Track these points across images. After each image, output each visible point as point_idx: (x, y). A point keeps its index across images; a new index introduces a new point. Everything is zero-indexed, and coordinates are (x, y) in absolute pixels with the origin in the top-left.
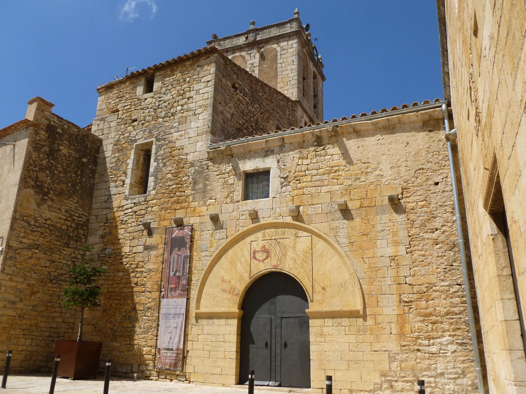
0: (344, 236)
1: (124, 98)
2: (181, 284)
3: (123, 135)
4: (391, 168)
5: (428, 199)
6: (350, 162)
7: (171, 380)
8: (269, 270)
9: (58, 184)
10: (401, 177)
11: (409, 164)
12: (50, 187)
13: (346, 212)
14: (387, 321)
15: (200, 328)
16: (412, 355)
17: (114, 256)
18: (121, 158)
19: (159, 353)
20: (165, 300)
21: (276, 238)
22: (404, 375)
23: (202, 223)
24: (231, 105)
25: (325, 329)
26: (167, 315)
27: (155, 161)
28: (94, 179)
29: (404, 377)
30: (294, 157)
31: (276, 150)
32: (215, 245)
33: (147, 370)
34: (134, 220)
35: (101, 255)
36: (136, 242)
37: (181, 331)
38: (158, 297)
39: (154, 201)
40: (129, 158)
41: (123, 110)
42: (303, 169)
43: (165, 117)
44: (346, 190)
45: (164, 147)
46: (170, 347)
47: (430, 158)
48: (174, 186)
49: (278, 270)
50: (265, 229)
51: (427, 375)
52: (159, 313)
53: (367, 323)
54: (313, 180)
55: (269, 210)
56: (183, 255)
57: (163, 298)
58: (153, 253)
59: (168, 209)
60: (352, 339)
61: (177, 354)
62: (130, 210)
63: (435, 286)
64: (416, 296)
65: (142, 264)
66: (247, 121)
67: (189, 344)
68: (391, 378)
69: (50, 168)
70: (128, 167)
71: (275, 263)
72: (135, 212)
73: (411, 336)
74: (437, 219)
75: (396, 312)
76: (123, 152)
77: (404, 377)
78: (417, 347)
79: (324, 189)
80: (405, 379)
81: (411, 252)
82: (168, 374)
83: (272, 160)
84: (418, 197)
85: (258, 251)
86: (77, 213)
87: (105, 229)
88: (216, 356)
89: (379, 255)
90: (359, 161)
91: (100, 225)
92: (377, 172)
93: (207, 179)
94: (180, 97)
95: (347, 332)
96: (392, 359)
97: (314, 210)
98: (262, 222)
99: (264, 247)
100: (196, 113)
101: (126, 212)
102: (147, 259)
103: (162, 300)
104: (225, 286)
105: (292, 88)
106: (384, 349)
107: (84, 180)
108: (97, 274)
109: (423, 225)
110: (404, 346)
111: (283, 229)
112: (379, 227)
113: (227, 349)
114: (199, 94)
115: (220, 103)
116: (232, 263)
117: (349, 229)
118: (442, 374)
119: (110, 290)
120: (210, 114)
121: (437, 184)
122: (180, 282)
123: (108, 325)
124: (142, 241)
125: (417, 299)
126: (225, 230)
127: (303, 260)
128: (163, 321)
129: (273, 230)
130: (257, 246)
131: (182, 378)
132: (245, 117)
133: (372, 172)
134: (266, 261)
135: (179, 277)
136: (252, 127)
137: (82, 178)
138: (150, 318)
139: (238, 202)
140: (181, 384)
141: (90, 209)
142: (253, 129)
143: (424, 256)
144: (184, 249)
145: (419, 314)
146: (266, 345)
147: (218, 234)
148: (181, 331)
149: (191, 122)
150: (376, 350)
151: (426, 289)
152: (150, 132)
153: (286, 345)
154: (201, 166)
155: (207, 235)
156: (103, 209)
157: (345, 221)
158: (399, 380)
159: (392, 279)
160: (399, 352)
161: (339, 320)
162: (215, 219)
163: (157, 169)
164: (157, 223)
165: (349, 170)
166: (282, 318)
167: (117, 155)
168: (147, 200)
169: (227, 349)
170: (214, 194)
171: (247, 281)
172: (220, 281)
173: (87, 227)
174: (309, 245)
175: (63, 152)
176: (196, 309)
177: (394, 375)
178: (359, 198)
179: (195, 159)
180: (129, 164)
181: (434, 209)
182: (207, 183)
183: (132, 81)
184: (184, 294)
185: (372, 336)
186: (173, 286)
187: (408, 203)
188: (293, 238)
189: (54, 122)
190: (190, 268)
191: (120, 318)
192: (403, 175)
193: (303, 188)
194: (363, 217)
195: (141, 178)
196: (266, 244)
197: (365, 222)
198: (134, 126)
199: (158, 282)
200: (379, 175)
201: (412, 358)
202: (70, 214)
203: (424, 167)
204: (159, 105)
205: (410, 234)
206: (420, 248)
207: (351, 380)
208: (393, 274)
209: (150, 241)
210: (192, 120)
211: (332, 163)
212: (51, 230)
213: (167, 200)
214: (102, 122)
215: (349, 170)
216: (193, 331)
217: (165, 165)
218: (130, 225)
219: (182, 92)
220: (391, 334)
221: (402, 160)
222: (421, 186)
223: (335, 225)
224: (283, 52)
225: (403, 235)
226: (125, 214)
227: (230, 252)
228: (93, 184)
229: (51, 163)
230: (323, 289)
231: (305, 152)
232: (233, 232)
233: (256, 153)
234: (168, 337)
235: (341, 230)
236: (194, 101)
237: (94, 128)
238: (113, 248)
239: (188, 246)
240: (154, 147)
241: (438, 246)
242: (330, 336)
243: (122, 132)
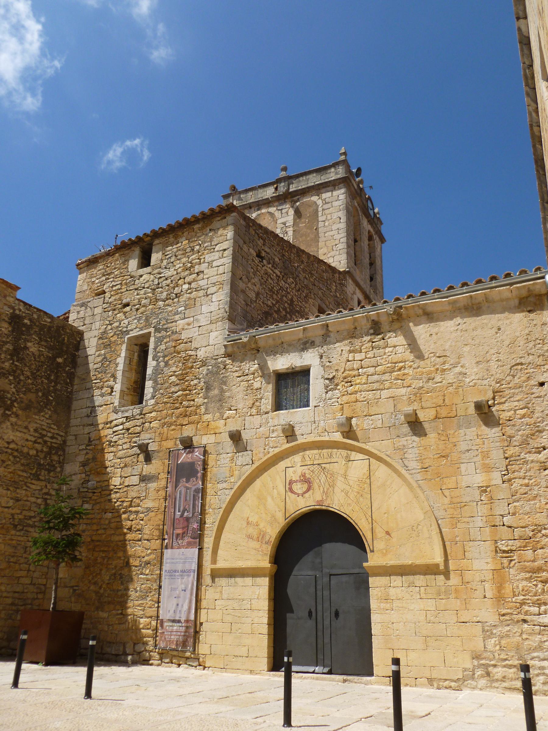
0: (414, 459)
1: (113, 276)
2: (190, 528)
3: (111, 324)
4: (477, 362)
5: (530, 405)
6: (420, 356)
7: (179, 665)
8: (312, 507)
9: (24, 394)
10: (492, 375)
11: (501, 357)
12: (14, 399)
13: (416, 426)
14: (478, 579)
15: (218, 590)
16: (516, 629)
17: (100, 490)
18: (108, 356)
19: (162, 626)
20: (169, 551)
21: (320, 462)
22: (505, 657)
23: (218, 443)
24: (256, 280)
27: (153, 360)
28: (72, 386)
29: (506, 660)
30: (342, 350)
31: (318, 341)
32: (236, 473)
34: (126, 440)
35: (82, 490)
36: (128, 470)
38: (160, 547)
40: (119, 356)
41: (111, 292)
42: (355, 367)
43: (167, 299)
44: (415, 394)
45: (165, 340)
46: (177, 618)
47: (531, 349)
48: (180, 393)
49: (324, 508)
50: (305, 450)
51: (538, 657)
52: (161, 569)
53: (451, 582)
54: (369, 381)
55: (310, 424)
57: (166, 548)
58: (153, 485)
59: (171, 424)
60: (430, 604)
61: (187, 627)
62: (121, 427)
63: (545, 529)
64: (518, 543)
65: (137, 501)
66: (277, 302)
67: (203, 612)
68: (488, 662)
69: (15, 372)
70: (118, 369)
72: (128, 429)
73: (514, 600)
74: (544, 434)
75: (491, 566)
76: (111, 348)
77: (506, 660)
78: (522, 617)
79: (385, 394)
80: (507, 662)
81: (510, 480)
82: (175, 656)
83: (313, 354)
84: (516, 404)
85: (296, 482)
86: (50, 432)
87: (87, 453)
88: (240, 631)
89: (464, 484)
90: (432, 355)
91: (81, 448)
92: (458, 369)
93: (225, 383)
94: (187, 272)
95: (423, 595)
96: (487, 634)
97: (371, 422)
98: (301, 440)
99: (304, 475)
100: (208, 293)
101: (115, 429)
102: (144, 494)
103: (165, 551)
104: (251, 530)
105: (339, 254)
106: (476, 620)
107: (59, 387)
108: (77, 516)
109: (525, 443)
110: (504, 615)
111: (330, 450)
112: (463, 446)
113: (256, 620)
114: (212, 267)
115: (241, 279)
116: (261, 498)
117: (421, 448)
119: (94, 538)
120: (227, 294)
121: (542, 384)
122: (189, 526)
123: (92, 587)
124: (137, 469)
125: (520, 547)
126: (250, 452)
127: (358, 493)
128: (167, 580)
130: (294, 474)
131: (193, 662)
132: (275, 297)
133: (450, 369)
134: (307, 495)
135: (187, 519)
136: (285, 309)
137: (56, 384)
138: (149, 577)
140: (192, 670)
141: (68, 426)
142: (286, 312)
143: (527, 485)
144: (195, 479)
145: (524, 569)
146: (310, 613)
147: (240, 458)
148: (191, 594)
149: (201, 305)
150: (464, 621)
151: (532, 533)
152: (147, 320)
153: (337, 614)
154: (216, 365)
155: (225, 459)
156: (84, 426)
157: (415, 438)
158: (499, 664)
159: (484, 519)
160: (498, 623)
161: (411, 578)
162: (236, 437)
163: (157, 371)
164: (157, 444)
165: (419, 367)
166: (331, 575)
167: (103, 352)
168: (144, 412)
169: (256, 620)
172: (245, 524)
173: (64, 451)
174: (365, 471)
175: (31, 350)
176: (212, 564)
177: (492, 656)
178: (434, 405)
180: (118, 363)
181: (539, 420)
182: (225, 387)
183: (122, 253)
184: (195, 543)
185: (458, 601)
186: (179, 531)
187: (502, 411)
188: (344, 462)
189: (20, 310)
190: (203, 506)
191: (108, 578)
192: (494, 373)
193: (356, 392)
194: (440, 432)
195: (135, 382)
196: (307, 472)
197: (443, 438)
198: (125, 313)
199: (159, 525)
200: (460, 373)
201: (515, 633)
202: (40, 434)
203: (523, 360)
204: (159, 284)
205: (506, 455)
206: (522, 474)
207: (431, 664)
208: (485, 512)
209: (148, 469)
210: (203, 302)
211: (395, 358)
212: (15, 457)
213: (170, 412)
214: (83, 308)
215: (419, 367)
216: (209, 594)
217: (167, 364)
218: (120, 447)
219: (189, 265)
220: (485, 597)
221: (493, 351)
222: (520, 387)
223: (401, 444)
224: (326, 206)
225: (497, 456)
226: (114, 432)
227: (258, 483)
228: (71, 392)
229: (16, 365)
230: (388, 533)
231: (357, 343)
232: (261, 455)
233: (290, 345)
234: (174, 603)
235: (410, 451)
236: (205, 277)
237: (72, 317)
238: (98, 479)
239: (199, 475)
240: (152, 340)
242: (398, 601)
243: (109, 321)
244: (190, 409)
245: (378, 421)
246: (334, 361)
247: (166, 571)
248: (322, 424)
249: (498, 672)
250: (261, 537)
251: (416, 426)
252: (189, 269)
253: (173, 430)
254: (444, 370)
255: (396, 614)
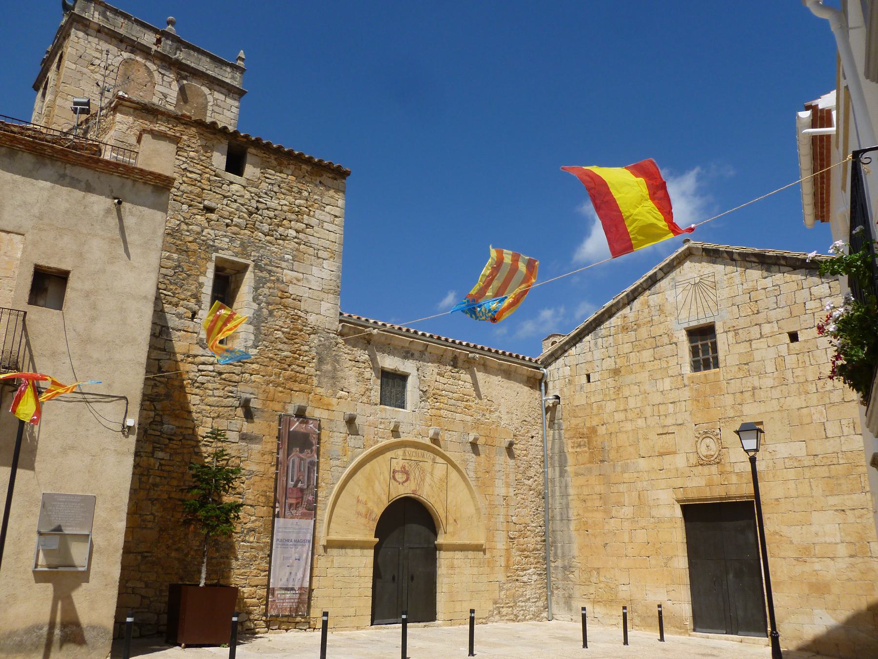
6: (479, 396)
7: (287, 630)
13: (474, 445)
15: (330, 559)
19: (273, 595)
20: (281, 520)
23: (332, 420)
25: (455, 562)
26: (285, 542)
31: (417, 354)
33: (250, 620)
34: (219, 386)
35: (150, 432)
37: (306, 564)
39: (255, 366)
40: (204, 274)
45: (268, 284)
46: (290, 586)
50: (406, 446)
53: (485, 557)
56: (308, 460)
58: (256, 447)
60: (475, 570)
61: (300, 594)
62: (211, 368)
70: (203, 290)
71: (413, 488)
72: (220, 374)
75: (504, 547)
78: (516, 578)
79: (458, 416)
96: (501, 589)
98: (404, 437)
99: (404, 467)
101: (201, 367)
112: (497, 468)
116: (370, 481)
118: (529, 599)
119: (173, 495)
121: (532, 437)
122: (297, 495)
123: (173, 554)
129: (413, 450)
130: (397, 464)
134: (406, 484)
135: (302, 490)
138: (255, 545)
139: (376, 404)
140: (303, 634)
145: (519, 550)
148: (306, 564)
153: (412, 578)
162: (350, 421)
169: (363, 585)
170: (346, 385)
171: (385, 504)
179: (318, 324)
183: (201, 132)
184: (311, 514)
186: (293, 501)
187: (517, 449)
190: (317, 477)
193: (440, 409)
216: (321, 563)
217: (271, 313)
225: (512, 477)
226: (199, 370)
227: (368, 466)
231: (443, 368)
232: (371, 442)
233: (395, 349)
234: (287, 573)
238: (177, 424)
239: (314, 448)
241: (531, 492)
244: (301, 376)
245: (455, 436)
246: (428, 378)
247: (277, 540)
248: (418, 427)
249: (504, 611)
250: (368, 514)
251: (474, 445)
252: (298, 213)
253: (281, 392)
254: (491, 411)
255: (453, 577)
